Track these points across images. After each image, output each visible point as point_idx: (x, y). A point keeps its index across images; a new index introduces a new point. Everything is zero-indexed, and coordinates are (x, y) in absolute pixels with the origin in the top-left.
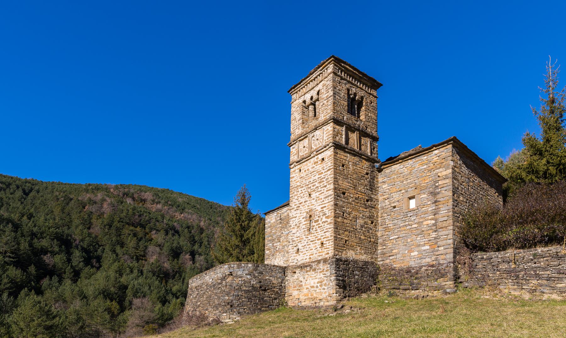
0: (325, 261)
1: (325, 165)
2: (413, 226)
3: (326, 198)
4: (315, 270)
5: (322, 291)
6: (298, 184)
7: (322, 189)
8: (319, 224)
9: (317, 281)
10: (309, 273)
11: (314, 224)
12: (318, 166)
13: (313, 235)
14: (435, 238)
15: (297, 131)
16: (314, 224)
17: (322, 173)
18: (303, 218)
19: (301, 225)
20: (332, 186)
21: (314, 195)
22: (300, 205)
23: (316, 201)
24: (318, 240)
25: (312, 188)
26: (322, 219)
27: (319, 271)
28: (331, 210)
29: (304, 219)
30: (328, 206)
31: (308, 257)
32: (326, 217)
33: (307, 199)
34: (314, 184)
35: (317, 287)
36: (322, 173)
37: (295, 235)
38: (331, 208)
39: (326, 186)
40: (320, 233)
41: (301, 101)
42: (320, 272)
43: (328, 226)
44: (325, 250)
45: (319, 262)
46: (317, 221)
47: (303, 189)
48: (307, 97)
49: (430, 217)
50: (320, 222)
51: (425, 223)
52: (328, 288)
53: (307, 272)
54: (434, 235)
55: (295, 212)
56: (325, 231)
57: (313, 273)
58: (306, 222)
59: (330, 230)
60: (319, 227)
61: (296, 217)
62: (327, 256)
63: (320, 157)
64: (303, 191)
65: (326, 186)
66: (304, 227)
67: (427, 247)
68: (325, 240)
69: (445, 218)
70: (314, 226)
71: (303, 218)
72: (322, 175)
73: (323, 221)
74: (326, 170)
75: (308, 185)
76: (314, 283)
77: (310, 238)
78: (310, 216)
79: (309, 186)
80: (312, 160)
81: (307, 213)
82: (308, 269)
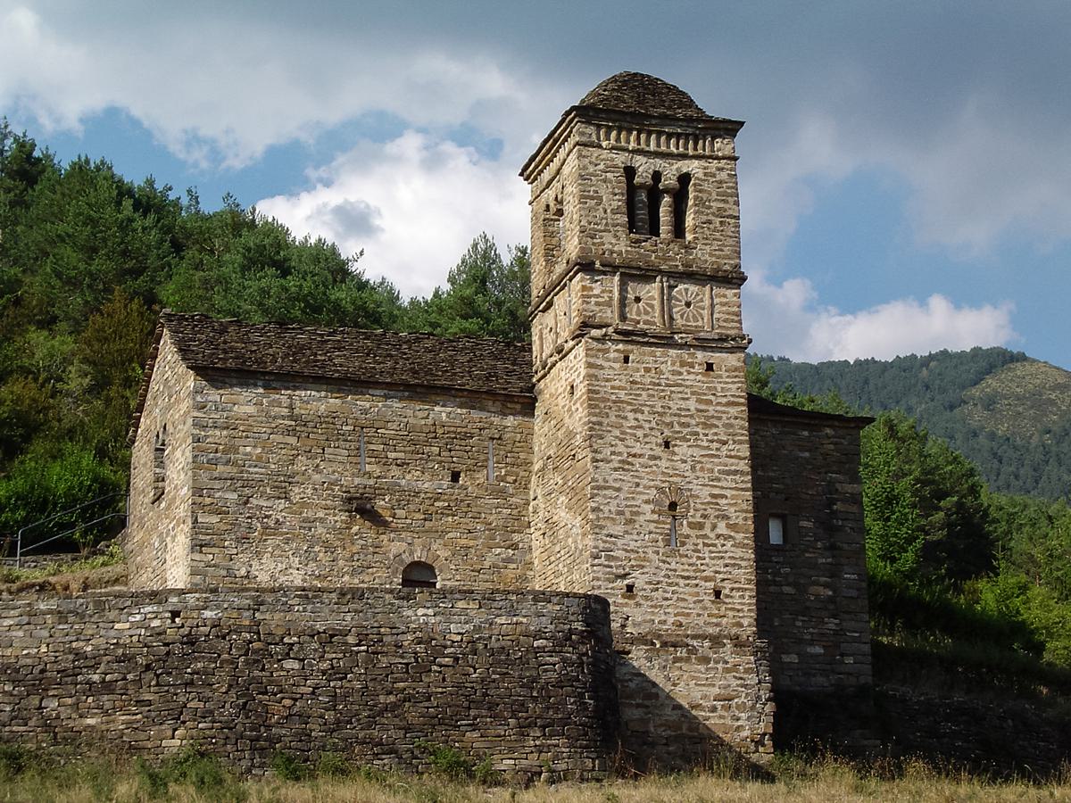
0: (738, 643)
1: (719, 387)
2: (787, 589)
3: (729, 473)
4: (706, 660)
5: (729, 722)
6: (622, 394)
7: (715, 445)
8: (705, 536)
9: (716, 691)
10: (685, 666)
11: (685, 530)
12: (692, 377)
13: (684, 560)
14: (836, 633)
15: (608, 238)
16: (685, 530)
17: (709, 402)
18: (647, 502)
19: (641, 518)
20: (745, 451)
21: (682, 450)
22: (636, 461)
23: (693, 468)
24: (707, 579)
25: (677, 428)
26: (714, 527)
27: (720, 666)
28: (746, 511)
29: (652, 506)
30: (733, 497)
31: (671, 620)
32: (728, 526)
33: (659, 451)
34: (683, 420)
35: (714, 709)
36: (709, 402)
37: (620, 542)
38: (745, 506)
39: (725, 443)
40: (707, 560)
41: (621, 159)
42: (727, 671)
43: (739, 553)
44: (731, 614)
45: (716, 641)
46: (701, 526)
47: (639, 416)
48: (645, 168)
49: (823, 579)
50: (707, 531)
51: (813, 589)
52: (749, 719)
53: (676, 660)
54: (832, 624)
55: (616, 475)
56: (727, 561)
57: (702, 668)
58: (655, 517)
59: (743, 564)
60: (705, 545)
61: (618, 490)
62: (734, 631)
63: (700, 356)
64: (647, 425)
65: (725, 443)
66: (652, 527)
67: (819, 650)
68: (728, 585)
69: (854, 593)
70: (688, 536)
71: (647, 502)
72: (711, 408)
73: (719, 531)
74: (724, 400)
75: (660, 414)
76: (704, 697)
77: (673, 566)
78: (673, 506)
79: (668, 420)
80: (673, 352)
81: (660, 490)
82: (682, 653)
